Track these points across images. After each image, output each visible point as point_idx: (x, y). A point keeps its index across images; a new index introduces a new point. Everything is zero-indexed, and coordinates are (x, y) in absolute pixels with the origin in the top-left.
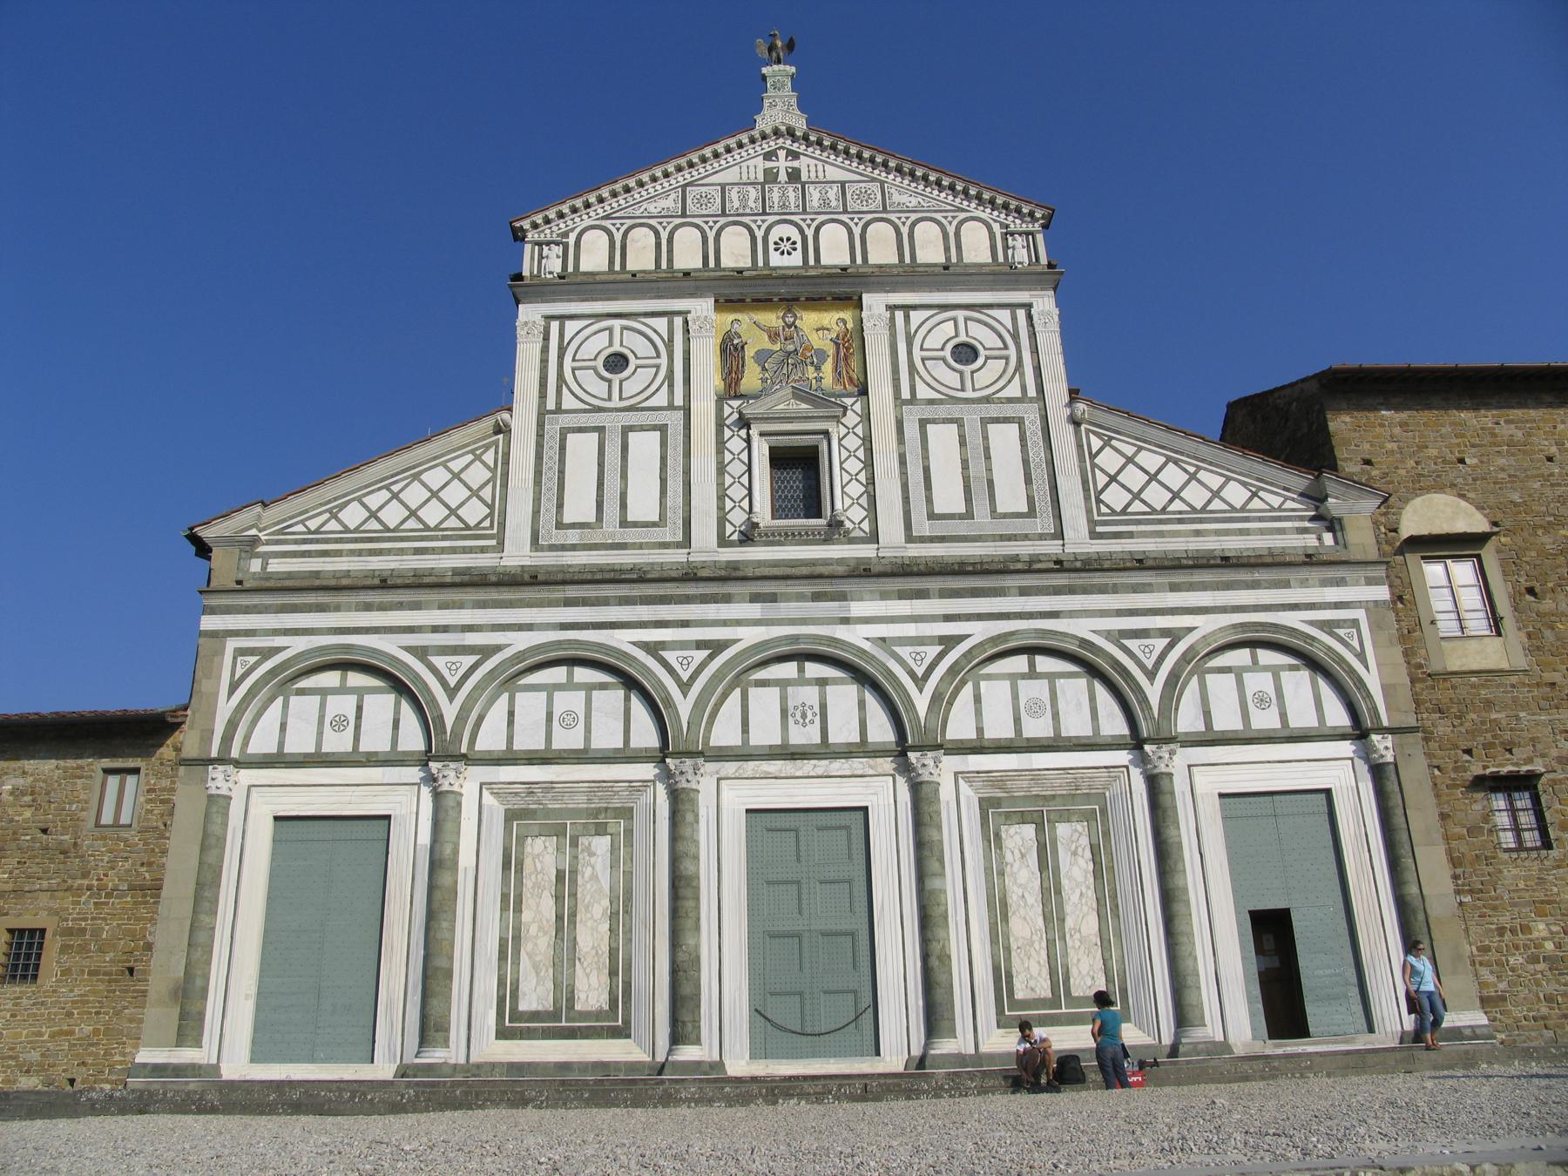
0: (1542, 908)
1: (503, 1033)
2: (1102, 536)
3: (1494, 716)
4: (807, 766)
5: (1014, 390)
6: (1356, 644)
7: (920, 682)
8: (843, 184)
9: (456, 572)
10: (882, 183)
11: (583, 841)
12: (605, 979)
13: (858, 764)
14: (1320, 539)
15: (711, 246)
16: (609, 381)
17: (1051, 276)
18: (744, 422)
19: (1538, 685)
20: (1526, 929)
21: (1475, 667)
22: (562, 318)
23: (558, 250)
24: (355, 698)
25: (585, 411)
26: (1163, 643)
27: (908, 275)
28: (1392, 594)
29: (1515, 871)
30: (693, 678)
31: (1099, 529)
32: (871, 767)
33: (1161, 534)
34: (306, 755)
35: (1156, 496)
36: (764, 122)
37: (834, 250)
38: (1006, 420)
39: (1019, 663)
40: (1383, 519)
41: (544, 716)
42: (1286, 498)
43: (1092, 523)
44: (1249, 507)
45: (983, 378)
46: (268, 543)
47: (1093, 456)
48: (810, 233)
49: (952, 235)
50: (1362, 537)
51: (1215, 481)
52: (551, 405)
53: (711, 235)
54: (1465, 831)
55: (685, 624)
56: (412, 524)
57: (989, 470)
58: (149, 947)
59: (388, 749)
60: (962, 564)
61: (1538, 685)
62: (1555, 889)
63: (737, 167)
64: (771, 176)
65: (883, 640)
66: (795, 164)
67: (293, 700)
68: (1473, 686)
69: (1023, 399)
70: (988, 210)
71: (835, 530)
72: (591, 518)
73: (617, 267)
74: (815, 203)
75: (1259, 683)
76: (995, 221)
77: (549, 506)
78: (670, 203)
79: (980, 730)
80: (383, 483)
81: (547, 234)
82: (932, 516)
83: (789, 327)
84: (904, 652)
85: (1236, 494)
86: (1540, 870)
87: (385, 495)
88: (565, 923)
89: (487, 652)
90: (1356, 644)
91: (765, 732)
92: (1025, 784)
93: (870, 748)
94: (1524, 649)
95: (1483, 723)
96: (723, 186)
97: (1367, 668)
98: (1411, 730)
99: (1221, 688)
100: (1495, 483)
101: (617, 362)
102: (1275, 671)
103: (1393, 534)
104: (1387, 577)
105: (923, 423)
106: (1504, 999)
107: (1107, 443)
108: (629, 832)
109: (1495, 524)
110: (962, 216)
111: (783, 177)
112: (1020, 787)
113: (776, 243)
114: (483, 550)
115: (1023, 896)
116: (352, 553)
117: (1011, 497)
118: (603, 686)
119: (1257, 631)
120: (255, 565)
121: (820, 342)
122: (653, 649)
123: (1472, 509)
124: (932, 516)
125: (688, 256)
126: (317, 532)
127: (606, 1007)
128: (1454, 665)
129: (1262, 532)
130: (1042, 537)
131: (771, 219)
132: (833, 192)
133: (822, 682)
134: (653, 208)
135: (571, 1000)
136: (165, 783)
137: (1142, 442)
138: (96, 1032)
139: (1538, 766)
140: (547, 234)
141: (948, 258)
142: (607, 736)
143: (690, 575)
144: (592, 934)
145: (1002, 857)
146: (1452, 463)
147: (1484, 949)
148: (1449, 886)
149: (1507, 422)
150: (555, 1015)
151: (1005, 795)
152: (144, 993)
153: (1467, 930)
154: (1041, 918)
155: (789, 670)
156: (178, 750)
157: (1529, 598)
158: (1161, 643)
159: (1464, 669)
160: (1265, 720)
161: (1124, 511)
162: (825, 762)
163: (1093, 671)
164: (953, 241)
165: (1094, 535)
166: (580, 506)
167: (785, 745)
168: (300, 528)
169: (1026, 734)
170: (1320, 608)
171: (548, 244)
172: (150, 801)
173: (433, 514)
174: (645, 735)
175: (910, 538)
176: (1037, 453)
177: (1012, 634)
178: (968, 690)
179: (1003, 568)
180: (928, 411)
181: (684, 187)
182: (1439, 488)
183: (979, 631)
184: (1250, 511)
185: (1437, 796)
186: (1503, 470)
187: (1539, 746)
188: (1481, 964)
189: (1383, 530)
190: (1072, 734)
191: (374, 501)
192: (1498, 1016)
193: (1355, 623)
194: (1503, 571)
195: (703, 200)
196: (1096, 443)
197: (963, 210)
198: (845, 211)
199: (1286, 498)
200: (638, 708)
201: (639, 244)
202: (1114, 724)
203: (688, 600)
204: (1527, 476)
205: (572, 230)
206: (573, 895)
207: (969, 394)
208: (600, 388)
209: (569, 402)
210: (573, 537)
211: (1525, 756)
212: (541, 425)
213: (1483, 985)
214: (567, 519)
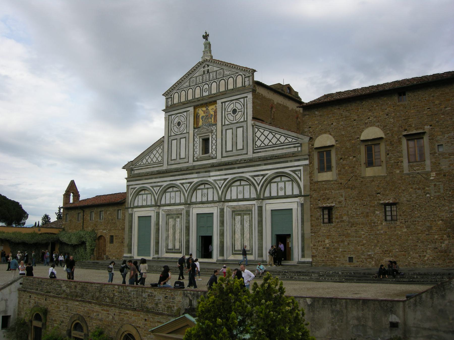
0: (328, 237)
1: (167, 252)
2: (255, 153)
3: (326, 192)
5: (242, 120)
6: (299, 175)
7: (220, 188)
8: (216, 71)
9: (157, 171)
10: (223, 69)
11: (176, 219)
12: (179, 243)
13: (212, 205)
14: (298, 149)
16: (178, 128)
19: (338, 184)
20: (324, 241)
21: (324, 179)
22: (171, 115)
23: (171, 99)
24: (146, 195)
25: (175, 135)
26: (261, 177)
28: (309, 162)
29: (324, 228)
30: (188, 189)
31: (255, 151)
32: (214, 205)
33: (266, 151)
34: (141, 206)
35: (266, 142)
38: (240, 127)
39: (238, 183)
40: (311, 143)
41: (170, 197)
42: (293, 139)
43: (253, 150)
44: (284, 142)
45: (237, 117)
46: (134, 168)
47: (255, 134)
48: (210, 86)
49: (235, 80)
50: (306, 148)
51: (278, 136)
52: (170, 135)
53: (194, 90)
54: (315, 219)
55: (186, 179)
56: (152, 162)
57: (237, 139)
58: (124, 238)
59: (150, 204)
60: (229, 163)
61: (338, 184)
62: (332, 233)
63: (198, 72)
64: (204, 72)
65: (215, 180)
66: (208, 68)
67: (139, 196)
68: (323, 184)
69: (244, 121)
70: (242, 72)
72: (176, 158)
73: (179, 102)
74: (211, 78)
75: (281, 185)
76: (243, 74)
77: (170, 156)
79: (231, 197)
82: (226, 152)
83: (207, 109)
84: (218, 182)
85: (282, 139)
86: (330, 228)
87: (148, 157)
88: (174, 233)
89: (161, 186)
90: (299, 175)
91: (199, 200)
92: (238, 208)
93: (215, 201)
94: (337, 174)
95: (324, 193)
96: (196, 77)
97: (301, 181)
98: (308, 196)
99: (274, 186)
100: (339, 129)
101: (179, 124)
102: (285, 182)
103: (313, 146)
104: (309, 158)
105: (226, 130)
106: (316, 256)
107: (258, 130)
108: (182, 218)
109: (337, 141)
110: (237, 74)
111: (206, 72)
112: (238, 209)
113: (204, 90)
114: (161, 166)
115: (238, 230)
116: (145, 168)
118: (177, 191)
119: (280, 174)
122: (182, 184)
123: (332, 137)
124: (226, 152)
126: (140, 165)
127: (179, 248)
128: (319, 180)
129: (287, 148)
130: (244, 154)
131: (204, 84)
132: (215, 73)
133: (208, 188)
134: (185, 86)
135: (175, 247)
136: (124, 212)
137: (265, 129)
138: (120, 251)
139: (333, 205)
141: (234, 87)
143: (187, 169)
144: (177, 236)
145: (235, 222)
146: (330, 125)
147: (315, 245)
148: (310, 231)
149: (346, 111)
150: (172, 250)
151: (235, 210)
152: (124, 245)
153: (312, 241)
154: (240, 235)
156: (125, 206)
157: (342, 161)
158: (261, 177)
159: (322, 180)
160: (281, 193)
161: (260, 146)
162: (207, 204)
165: (254, 153)
167: (202, 201)
168: (138, 164)
169: (238, 198)
170: (291, 167)
171: (169, 98)
172: (123, 215)
173: (155, 160)
175: (222, 157)
177: (235, 177)
178: (230, 189)
179: (235, 162)
181: (190, 79)
182: (325, 133)
183: (230, 177)
184: (285, 143)
185: (311, 211)
186: (342, 125)
187: (335, 199)
188: (313, 249)
189: (310, 145)
190: (246, 198)
191: (147, 158)
192: (315, 260)
193: (300, 170)
194: (336, 154)
196: (256, 130)
197: (238, 73)
198: (216, 79)
199: (293, 139)
201: (182, 95)
203: (187, 174)
204: (348, 127)
205: (172, 94)
206: (175, 229)
207: (235, 122)
208: (176, 130)
210: (173, 162)
211: (331, 201)
212: (168, 139)
213: (313, 253)
214: (172, 159)
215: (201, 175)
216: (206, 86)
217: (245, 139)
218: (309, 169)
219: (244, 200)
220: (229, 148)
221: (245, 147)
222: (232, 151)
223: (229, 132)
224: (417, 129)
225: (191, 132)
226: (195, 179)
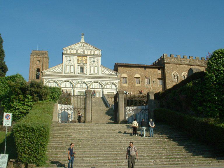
4: (81, 89)
7: (89, 84)
15: (77, 52)
17: (101, 55)
18: (79, 66)
27: (91, 55)
35: (106, 73)
36: (81, 42)
37: (86, 53)
39: (95, 83)
50: (119, 76)
64: (81, 46)
71: (84, 74)
75: (110, 85)
77: (65, 71)
78: (74, 48)
80: (54, 68)
81: (65, 50)
85: (111, 73)
89: (62, 81)
91: (79, 87)
99: (108, 86)
117: (96, 72)
120: (46, 74)
121: (84, 60)
122: (72, 81)
125: (75, 52)
134: (73, 48)
140: (65, 50)
142: (69, 86)
155: (81, 83)
160: (110, 88)
163: (100, 84)
164: (94, 52)
166: (67, 71)
173: (58, 71)
174: (72, 86)
176: (98, 69)
180: (91, 66)
183: (93, 81)
191: (54, 69)
195: (76, 48)
200: (71, 85)
202: (101, 87)
209: (67, 63)
210: (67, 73)
214: (67, 72)
215: (81, 79)
216: (82, 51)
217: (98, 70)
218: (120, 83)
219: (97, 88)
220: (92, 72)
221: (98, 73)
222: (93, 73)
223: (92, 68)
224: (148, 77)
225: (76, 64)
226: (78, 80)
